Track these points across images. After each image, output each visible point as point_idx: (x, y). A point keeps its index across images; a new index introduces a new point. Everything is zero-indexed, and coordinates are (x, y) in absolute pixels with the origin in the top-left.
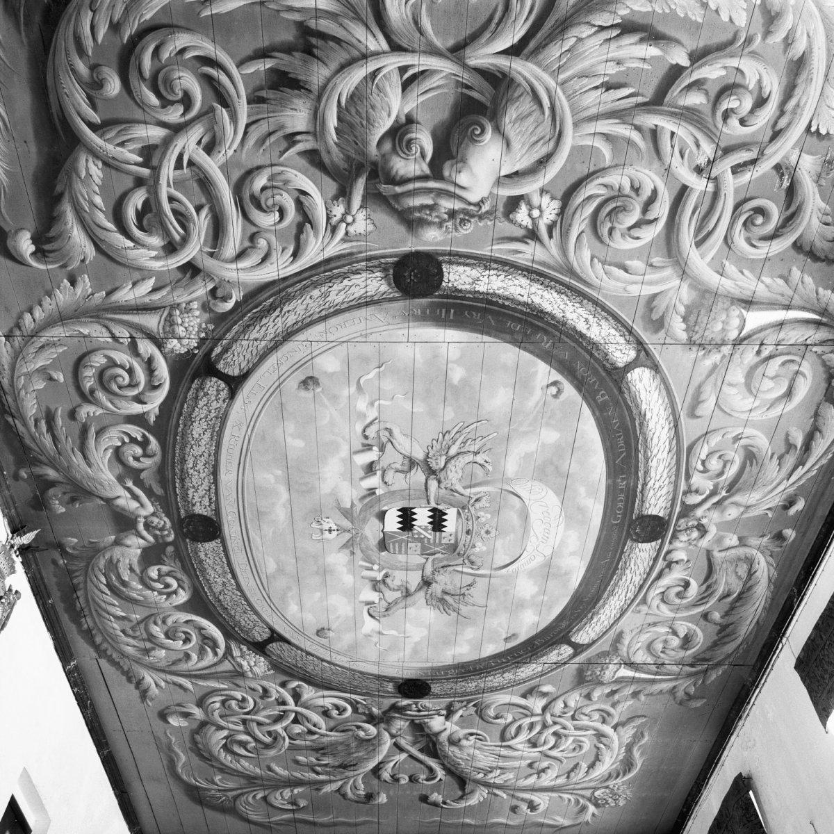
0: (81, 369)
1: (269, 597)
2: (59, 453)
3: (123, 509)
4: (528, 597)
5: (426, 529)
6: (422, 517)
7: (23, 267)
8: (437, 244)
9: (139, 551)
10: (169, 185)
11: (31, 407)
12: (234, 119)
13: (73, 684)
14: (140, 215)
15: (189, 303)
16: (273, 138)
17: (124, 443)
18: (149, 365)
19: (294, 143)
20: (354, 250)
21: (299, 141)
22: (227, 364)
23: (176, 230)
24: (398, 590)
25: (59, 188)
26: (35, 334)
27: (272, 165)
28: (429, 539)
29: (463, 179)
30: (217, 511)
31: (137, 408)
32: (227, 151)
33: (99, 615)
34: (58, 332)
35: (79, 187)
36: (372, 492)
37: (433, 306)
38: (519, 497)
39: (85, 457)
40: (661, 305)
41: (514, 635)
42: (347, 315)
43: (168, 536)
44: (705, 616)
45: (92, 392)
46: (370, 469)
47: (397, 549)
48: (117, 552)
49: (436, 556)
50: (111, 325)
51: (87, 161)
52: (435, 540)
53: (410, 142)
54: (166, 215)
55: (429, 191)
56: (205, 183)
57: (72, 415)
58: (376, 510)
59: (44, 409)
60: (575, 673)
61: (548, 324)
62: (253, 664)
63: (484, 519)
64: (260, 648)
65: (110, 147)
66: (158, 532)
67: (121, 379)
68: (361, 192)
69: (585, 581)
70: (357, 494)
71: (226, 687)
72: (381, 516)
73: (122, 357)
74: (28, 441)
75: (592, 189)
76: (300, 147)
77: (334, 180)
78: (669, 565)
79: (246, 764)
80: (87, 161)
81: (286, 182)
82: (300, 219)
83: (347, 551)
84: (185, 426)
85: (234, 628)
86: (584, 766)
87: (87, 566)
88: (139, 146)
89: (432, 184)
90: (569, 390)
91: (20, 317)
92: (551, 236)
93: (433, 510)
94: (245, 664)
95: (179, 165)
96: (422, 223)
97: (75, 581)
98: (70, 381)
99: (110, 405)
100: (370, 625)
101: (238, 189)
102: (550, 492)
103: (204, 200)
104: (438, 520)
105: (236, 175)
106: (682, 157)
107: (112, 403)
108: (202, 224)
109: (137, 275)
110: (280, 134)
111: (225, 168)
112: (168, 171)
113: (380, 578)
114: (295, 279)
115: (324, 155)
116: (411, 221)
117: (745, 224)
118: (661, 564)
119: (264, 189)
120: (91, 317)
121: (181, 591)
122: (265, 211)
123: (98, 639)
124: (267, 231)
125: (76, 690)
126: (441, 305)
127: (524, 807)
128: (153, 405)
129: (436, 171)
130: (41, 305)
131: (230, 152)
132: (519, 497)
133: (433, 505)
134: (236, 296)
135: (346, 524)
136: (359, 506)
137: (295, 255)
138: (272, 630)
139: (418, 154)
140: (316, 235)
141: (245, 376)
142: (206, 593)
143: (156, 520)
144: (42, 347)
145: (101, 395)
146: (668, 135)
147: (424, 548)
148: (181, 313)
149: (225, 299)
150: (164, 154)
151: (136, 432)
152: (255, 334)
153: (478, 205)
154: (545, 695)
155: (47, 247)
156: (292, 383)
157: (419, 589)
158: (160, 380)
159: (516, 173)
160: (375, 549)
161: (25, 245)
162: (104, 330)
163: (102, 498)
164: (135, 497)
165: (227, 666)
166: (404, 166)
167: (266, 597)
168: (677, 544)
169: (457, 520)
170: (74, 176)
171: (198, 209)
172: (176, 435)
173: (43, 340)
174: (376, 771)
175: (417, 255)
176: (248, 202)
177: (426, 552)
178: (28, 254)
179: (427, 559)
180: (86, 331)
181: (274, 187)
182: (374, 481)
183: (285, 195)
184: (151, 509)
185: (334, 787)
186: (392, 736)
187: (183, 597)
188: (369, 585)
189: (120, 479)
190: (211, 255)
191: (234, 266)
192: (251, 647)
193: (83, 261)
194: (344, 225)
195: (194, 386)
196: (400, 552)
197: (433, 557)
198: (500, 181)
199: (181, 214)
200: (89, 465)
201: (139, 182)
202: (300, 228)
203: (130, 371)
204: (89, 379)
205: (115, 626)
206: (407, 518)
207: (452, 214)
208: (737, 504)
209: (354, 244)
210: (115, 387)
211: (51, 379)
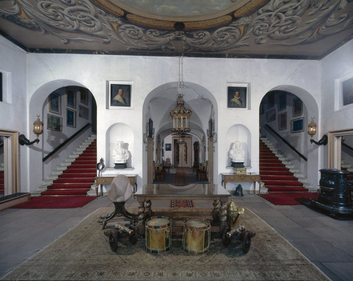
9: (188, 38)
10: (77, 18)
12: (52, 4)
17: (152, 35)
30: (174, 22)
34: (125, 39)
62: (243, 21)
66: (181, 34)
79: (299, 29)
85: (223, 24)
107: (140, 35)
123: (220, 49)
134: (99, 9)
141: (124, 10)
143: (176, 34)
149: (101, 12)
152: (108, 6)
164: (169, 36)
165: (242, 28)
172: (147, 26)
184: (173, 34)
187: (207, 33)
191: (90, 9)
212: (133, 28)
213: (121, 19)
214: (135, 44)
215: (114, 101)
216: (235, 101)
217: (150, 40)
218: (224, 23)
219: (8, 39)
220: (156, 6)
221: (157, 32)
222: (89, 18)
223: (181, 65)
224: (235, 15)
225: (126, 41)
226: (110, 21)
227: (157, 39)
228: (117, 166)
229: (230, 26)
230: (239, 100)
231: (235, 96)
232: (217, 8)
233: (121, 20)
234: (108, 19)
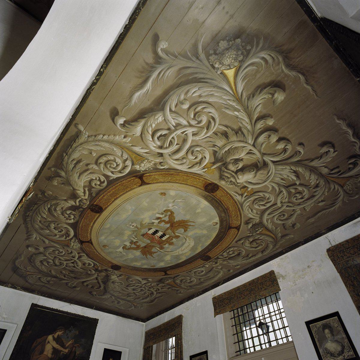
0: (103, 156)
1: (98, 233)
2: (72, 171)
3: (77, 194)
4: (166, 260)
7: (114, 125)
8: (222, 185)
10: (176, 135)
11: (76, 155)
12: (206, 133)
14: (161, 136)
15: (152, 161)
16: (210, 143)
17: (96, 179)
18: (124, 167)
19: (214, 147)
20: (204, 175)
21: (215, 147)
22: (146, 179)
23: (167, 144)
25: (146, 116)
26: (99, 141)
27: (204, 148)
29: (240, 177)
31: (110, 174)
32: (197, 138)
33: (37, 214)
34: (107, 145)
35: (152, 119)
36: (153, 223)
37: (208, 196)
39: (79, 176)
40: (251, 220)
41: (154, 266)
42: (188, 186)
43: (84, 206)
44: (200, 279)
45: (100, 163)
47: (146, 237)
48: (63, 202)
50: (124, 152)
51: (161, 116)
53: (238, 163)
54: (168, 140)
55: (231, 174)
56: (185, 141)
57: (87, 165)
58: (150, 227)
59: (80, 158)
60: (160, 279)
61: (227, 212)
64: (82, 242)
65: (170, 117)
67: (113, 165)
68: (217, 166)
69: (182, 262)
71: (59, 247)
72: (150, 229)
73: (119, 161)
74: (64, 163)
75: (261, 194)
76: (214, 149)
77: (215, 160)
78: (203, 267)
80: (161, 116)
81: (204, 153)
82: (199, 162)
83: (132, 232)
84: (119, 185)
86: (141, 298)
87: (47, 201)
88: (177, 122)
89: (233, 174)
91: (99, 135)
92: (245, 197)
94: (72, 244)
95: (183, 133)
96: (223, 179)
98: (97, 157)
99: (102, 169)
100: (121, 249)
101: (191, 147)
103: (181, 144)
105: (194, 144)
106: (281, 198)
107: (103, 169)
108: (175, 147)
109: (145, 147)
110: (213, 143)
111: (193, 141)
112: (179, 132)
114: (184, 172)
115: (218, 154)
116: (221, 178)
117: (279, 216)
118: (202, 265)
119: (197, 151)
120: (121, 147)
121: (73, 220)
122: (193, 155)
124: (188, 159)
126: (210, 196)
127: (116, 302)
128: (115, 176)
129: (236, 172)
130: (109, 136)
131: (198, 139)
136: (147, 224)
137: (189, 168)
138: (91, 240)
139: (237, 167)
140: (198, 167)
142: (80, 224)
144: (97, 145)
145: (102, 166)
146: (283, 194)
148: (147, 162)
149: (162, 166)
150: (182, 128)
151: (103, 178)
153: (238, 183)
154: (148, 280)
155: (127, 125)
156: (159, 192)
157: (143, 247)
158: (124, 172)
159: (251, 183)
161: (121, 121)
162: (121, 152)
163: (73, 188)
164: (85, 193)
166: (232, 167)
167: (98, 232)
168: (209, 264)
170: (154, 116)
171: (177, 144)
173: (99, 143)
174: (83, 282)
175: (216, 184)
176: (191, 150)
178: (119, 123)
180: (115, 149)
181: (200, 152)
182: (157, 221)
183: (201, 155)
184: (86, 197)
185: (66, 281)
186: (98, 276)
188: (130, 241)
189: (84, 187)
190: (170, 155)
191: (172, 161)
192: (79, 242)
193: (134, 135)
194: (207, 169)
195: (132, 178)
196: (146, 238)
198: (246, 182)
199: (172, 143)
200: (78, 179)
201: (169, 129)
202: (197, 163)
203: (117, 165)
204: (103, 160)
206: (156, 232)
207: (231, 181)
208: (227, 262)
209: (205, 174)
210: (108, 166)
211: (91, 153)
212: (120, 172)
213: (140, 172)
220: (134, 208)
222: (165, 146)
225: (103, 144)
226: (146, 161)
229: (73, 237)
233: (139, 171)
234: (150, 162)
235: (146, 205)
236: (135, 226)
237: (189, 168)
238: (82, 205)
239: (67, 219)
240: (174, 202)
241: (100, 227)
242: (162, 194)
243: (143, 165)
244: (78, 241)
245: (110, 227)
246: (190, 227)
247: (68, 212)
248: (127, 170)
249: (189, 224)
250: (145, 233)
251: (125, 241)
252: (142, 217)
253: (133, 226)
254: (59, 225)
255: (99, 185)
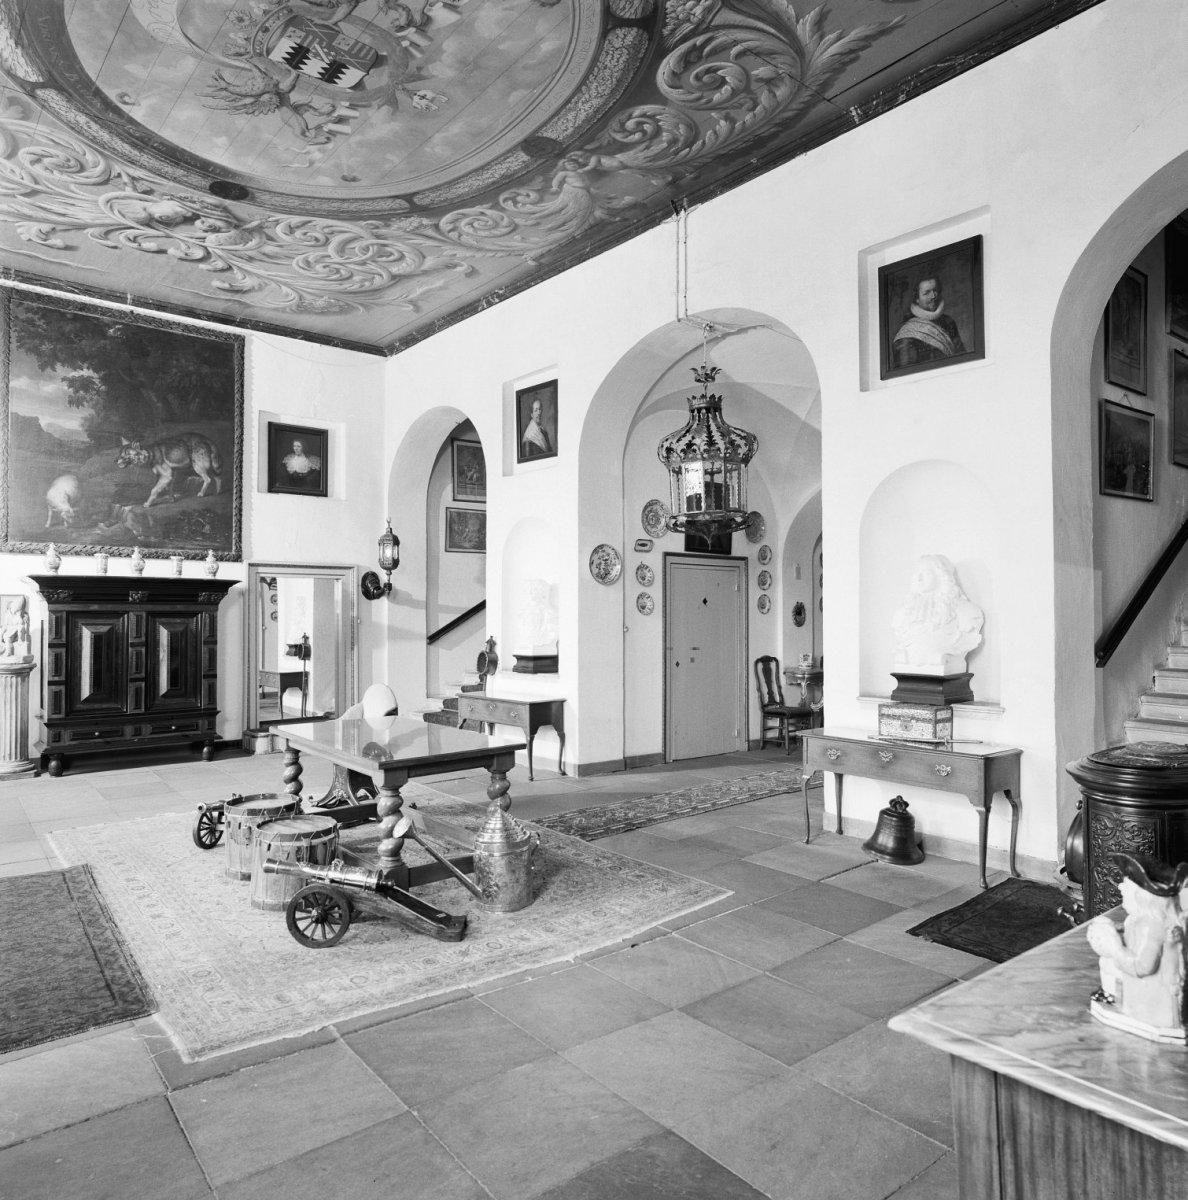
5: (317, 55)
6: (313, 67)
13: (890, 104)
18: (454, 221)
24: (399, 6)
28: (320, 44)
31: (489, 212)
33: (743, 131)
36: (352, 107)
38: (186, 36)
46: (341, 120)
47: (365, 51)
49: (322, 22)
52: (312, 42)
58: (358, 94)
63: (241, 35)
70: (370, 112)
72: (359, 86)
83: (424, 73)
85: (642, 59)
90: (112, 94)
93: (296, 67)
97: (709, 160)
102: (144, 24)
104: (297, 57)
113: (412, 30)
125: (902, 97)
132: (186, 36)
133: (294, 73)
135: (401, 96)
136: (375, 103)
142: (614, 103)
147: (332, 38)
149: (372, 224)
152: (366, 208)
160: (390, 62)
169: (274, 47)
177: (332, 32)
179: (336, 24)
182: (342, 111)
188: (431, 29)
189: (557, 193)
196: (364, 45)
197: (326, 23)
205: (748, 117)
206: (332, 73)
210: (490, 222)
214: (535, 245)
215: (525, 443)
216: (918, 336)
217: (540, 217)
218: (641, 55)
219: (336, 345)
220: (427, 149)
221: (522, 191)
223: (682, 246)
224: (627, 16)
227: (551, 205)
228: (523, 663)
230: (941, 322)
231: (916, 310)
232: (546, 47)
235: (389, 156)
236: (416, 98)
237: (310, 222)
238: (581, 156)
239: (652, 117)
240: (312, 163)
241: (544, 94)
242: (354, 179)
243: (415, 224)
244: (665, 25)
245: (510, 93)
246: (209, 90)
247: (637, 136)
248: (449, 217)
249: (223, 103)
250: (372, 71)
251: (455, 28)
252: (396, 126)
253: (423, 97)
254: (697, 95)
255: (518, 195)
